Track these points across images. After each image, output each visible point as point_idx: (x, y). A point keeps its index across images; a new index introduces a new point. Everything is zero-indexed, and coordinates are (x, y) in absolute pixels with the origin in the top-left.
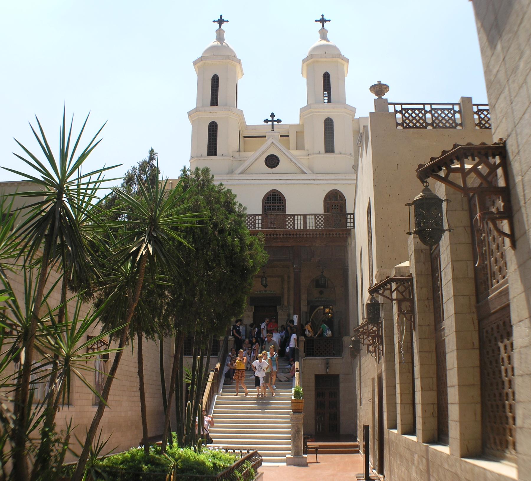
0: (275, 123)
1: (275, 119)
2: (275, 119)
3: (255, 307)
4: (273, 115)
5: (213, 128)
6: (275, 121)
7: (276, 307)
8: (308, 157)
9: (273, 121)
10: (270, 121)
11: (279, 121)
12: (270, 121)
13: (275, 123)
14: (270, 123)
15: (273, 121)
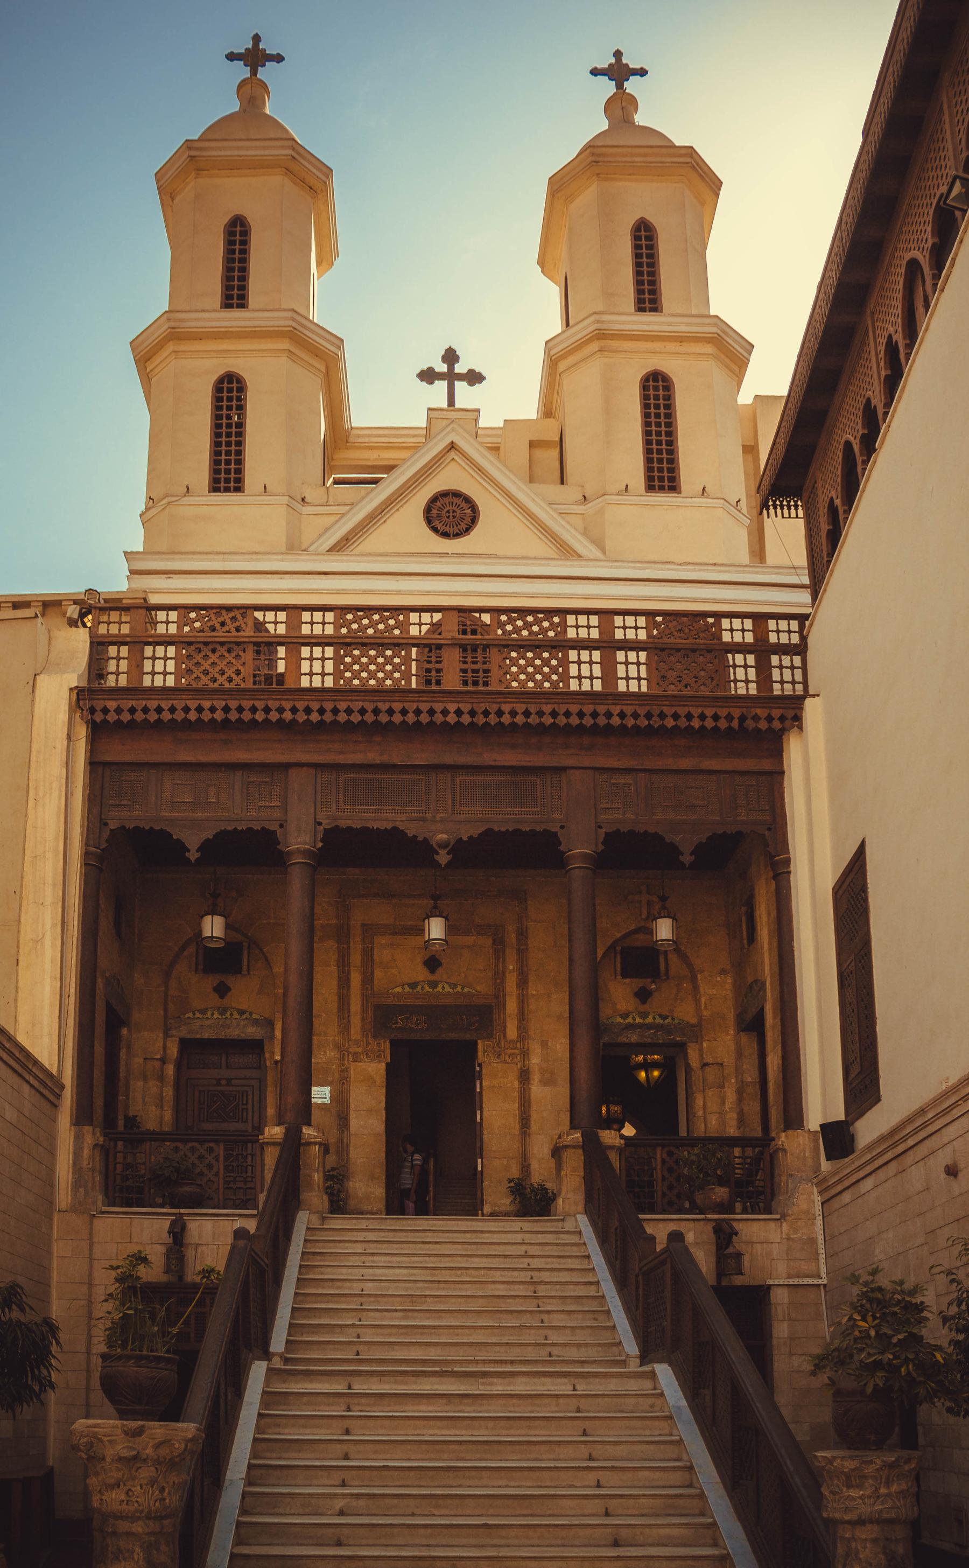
0: (460, 386)
1: (460, 368)
2: (460, 368)
3: (394, 1043)
4: (451, 357)
5: (230, 394)
6: (461, 377)
7: (475, 1044)
8: (580, 509)
9: (451, 377)
10: (441, 376)
11: (474, 378)
12: (441, 376)
13: (460, 386)
14: (442, 385)
15: (451, 377)
